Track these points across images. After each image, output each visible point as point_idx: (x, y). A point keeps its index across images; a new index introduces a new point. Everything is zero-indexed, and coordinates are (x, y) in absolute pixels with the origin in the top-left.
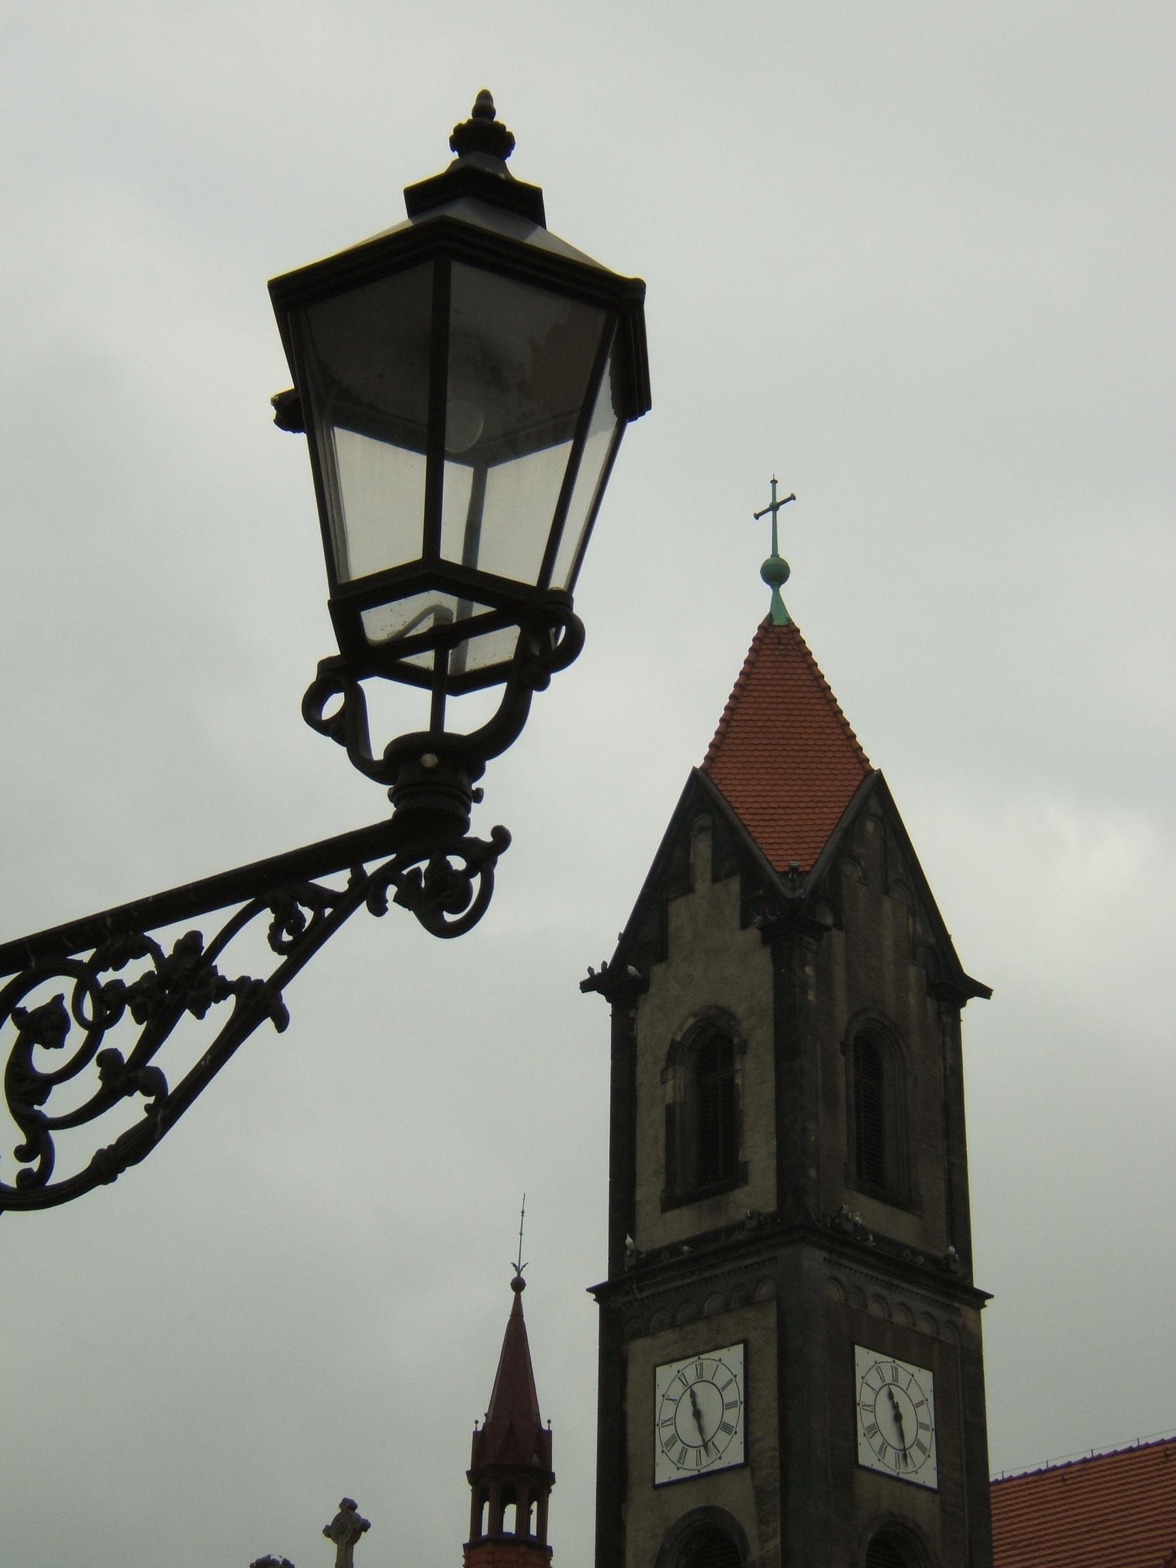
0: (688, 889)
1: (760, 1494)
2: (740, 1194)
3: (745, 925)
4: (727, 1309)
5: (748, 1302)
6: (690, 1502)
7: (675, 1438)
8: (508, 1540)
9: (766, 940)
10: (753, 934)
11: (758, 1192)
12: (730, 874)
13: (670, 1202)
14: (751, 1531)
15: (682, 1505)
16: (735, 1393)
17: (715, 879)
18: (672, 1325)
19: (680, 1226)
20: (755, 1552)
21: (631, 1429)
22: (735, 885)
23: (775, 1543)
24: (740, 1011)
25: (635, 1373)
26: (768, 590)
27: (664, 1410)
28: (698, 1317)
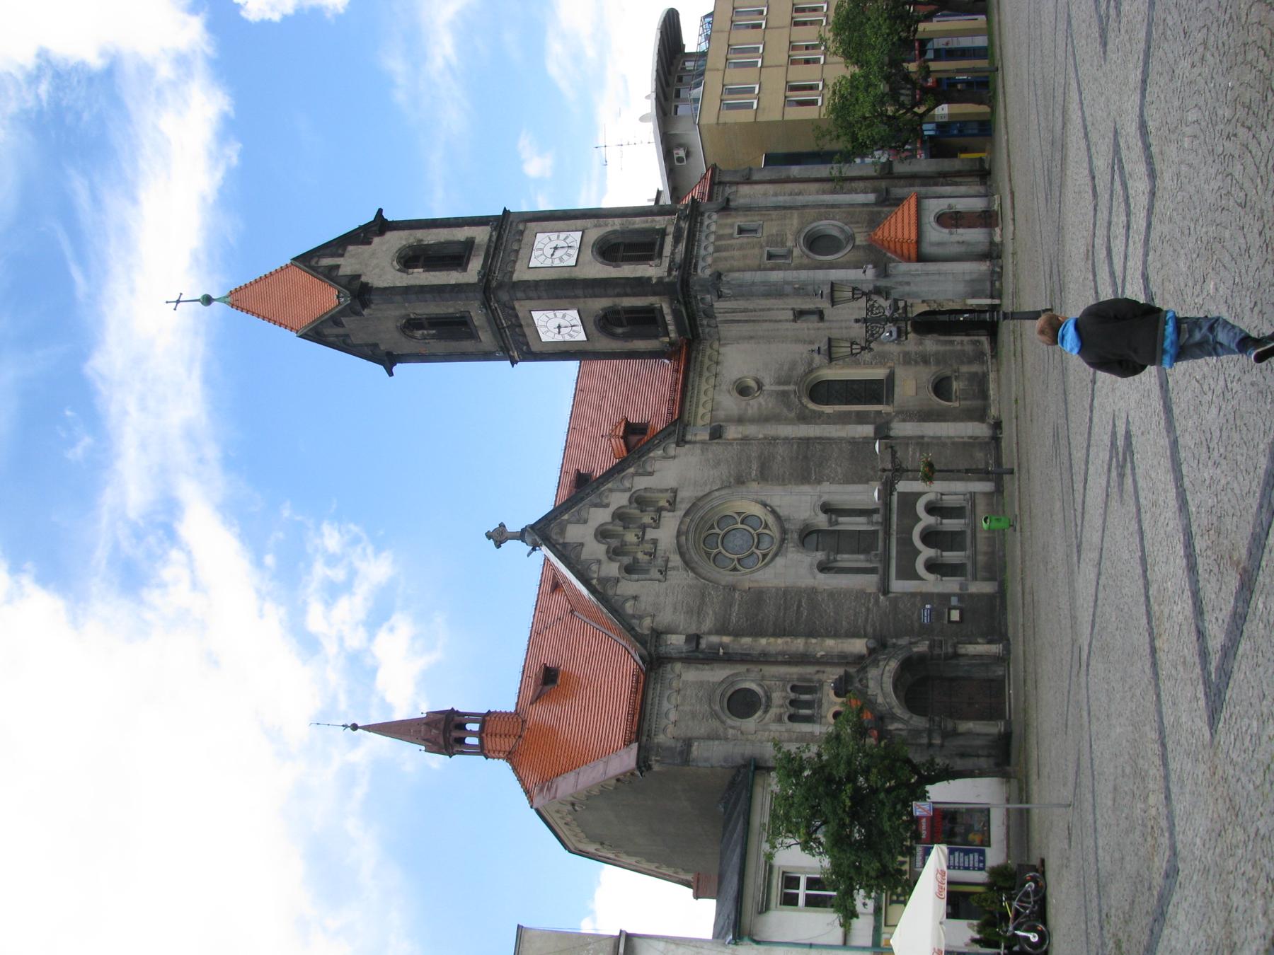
0: (338, 267)
1: (596, 226)
2: (477, 241)
3: (370, 243)
4: (520, 241)
5: (522, 233)
6: (588, 253)
7: (561, 259)
8: (482, 728)
9: (381, 233)
10: (376, 240)
11: (481, 235)
12: (345, 250)
13: (465, 270)
14: (609, 229)
15: (588, 254)
16: (554, 236)
17: (342, 255)
18: (515, 262)
19: (475, 265)
20: (617, 227)
21: (547, 278)
22: (351, 248)
23: (617, 221)
24: (404, 243)
25: (528, 276)
26: (215, 303)
27: (548, 263)
28: (517, 252)
